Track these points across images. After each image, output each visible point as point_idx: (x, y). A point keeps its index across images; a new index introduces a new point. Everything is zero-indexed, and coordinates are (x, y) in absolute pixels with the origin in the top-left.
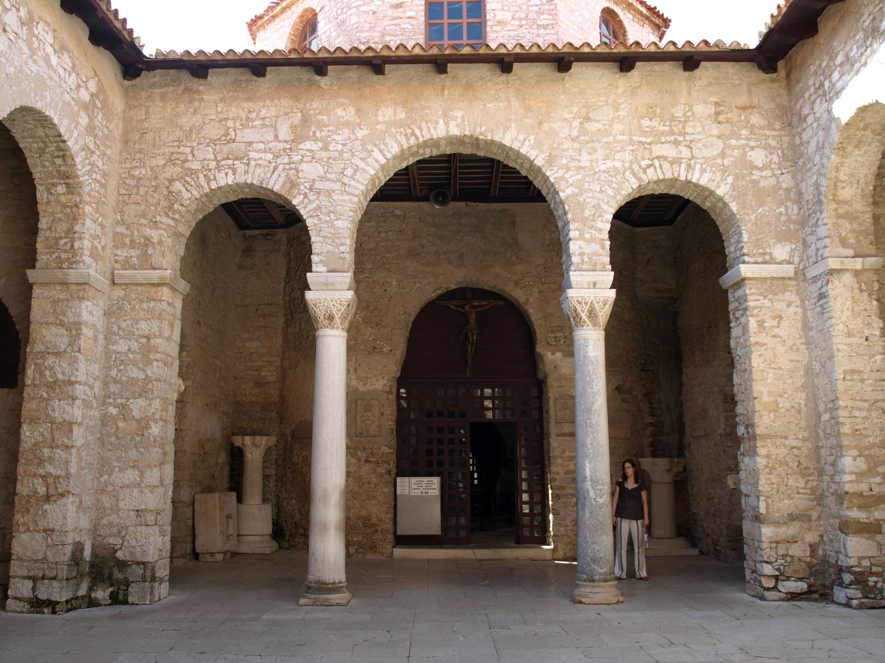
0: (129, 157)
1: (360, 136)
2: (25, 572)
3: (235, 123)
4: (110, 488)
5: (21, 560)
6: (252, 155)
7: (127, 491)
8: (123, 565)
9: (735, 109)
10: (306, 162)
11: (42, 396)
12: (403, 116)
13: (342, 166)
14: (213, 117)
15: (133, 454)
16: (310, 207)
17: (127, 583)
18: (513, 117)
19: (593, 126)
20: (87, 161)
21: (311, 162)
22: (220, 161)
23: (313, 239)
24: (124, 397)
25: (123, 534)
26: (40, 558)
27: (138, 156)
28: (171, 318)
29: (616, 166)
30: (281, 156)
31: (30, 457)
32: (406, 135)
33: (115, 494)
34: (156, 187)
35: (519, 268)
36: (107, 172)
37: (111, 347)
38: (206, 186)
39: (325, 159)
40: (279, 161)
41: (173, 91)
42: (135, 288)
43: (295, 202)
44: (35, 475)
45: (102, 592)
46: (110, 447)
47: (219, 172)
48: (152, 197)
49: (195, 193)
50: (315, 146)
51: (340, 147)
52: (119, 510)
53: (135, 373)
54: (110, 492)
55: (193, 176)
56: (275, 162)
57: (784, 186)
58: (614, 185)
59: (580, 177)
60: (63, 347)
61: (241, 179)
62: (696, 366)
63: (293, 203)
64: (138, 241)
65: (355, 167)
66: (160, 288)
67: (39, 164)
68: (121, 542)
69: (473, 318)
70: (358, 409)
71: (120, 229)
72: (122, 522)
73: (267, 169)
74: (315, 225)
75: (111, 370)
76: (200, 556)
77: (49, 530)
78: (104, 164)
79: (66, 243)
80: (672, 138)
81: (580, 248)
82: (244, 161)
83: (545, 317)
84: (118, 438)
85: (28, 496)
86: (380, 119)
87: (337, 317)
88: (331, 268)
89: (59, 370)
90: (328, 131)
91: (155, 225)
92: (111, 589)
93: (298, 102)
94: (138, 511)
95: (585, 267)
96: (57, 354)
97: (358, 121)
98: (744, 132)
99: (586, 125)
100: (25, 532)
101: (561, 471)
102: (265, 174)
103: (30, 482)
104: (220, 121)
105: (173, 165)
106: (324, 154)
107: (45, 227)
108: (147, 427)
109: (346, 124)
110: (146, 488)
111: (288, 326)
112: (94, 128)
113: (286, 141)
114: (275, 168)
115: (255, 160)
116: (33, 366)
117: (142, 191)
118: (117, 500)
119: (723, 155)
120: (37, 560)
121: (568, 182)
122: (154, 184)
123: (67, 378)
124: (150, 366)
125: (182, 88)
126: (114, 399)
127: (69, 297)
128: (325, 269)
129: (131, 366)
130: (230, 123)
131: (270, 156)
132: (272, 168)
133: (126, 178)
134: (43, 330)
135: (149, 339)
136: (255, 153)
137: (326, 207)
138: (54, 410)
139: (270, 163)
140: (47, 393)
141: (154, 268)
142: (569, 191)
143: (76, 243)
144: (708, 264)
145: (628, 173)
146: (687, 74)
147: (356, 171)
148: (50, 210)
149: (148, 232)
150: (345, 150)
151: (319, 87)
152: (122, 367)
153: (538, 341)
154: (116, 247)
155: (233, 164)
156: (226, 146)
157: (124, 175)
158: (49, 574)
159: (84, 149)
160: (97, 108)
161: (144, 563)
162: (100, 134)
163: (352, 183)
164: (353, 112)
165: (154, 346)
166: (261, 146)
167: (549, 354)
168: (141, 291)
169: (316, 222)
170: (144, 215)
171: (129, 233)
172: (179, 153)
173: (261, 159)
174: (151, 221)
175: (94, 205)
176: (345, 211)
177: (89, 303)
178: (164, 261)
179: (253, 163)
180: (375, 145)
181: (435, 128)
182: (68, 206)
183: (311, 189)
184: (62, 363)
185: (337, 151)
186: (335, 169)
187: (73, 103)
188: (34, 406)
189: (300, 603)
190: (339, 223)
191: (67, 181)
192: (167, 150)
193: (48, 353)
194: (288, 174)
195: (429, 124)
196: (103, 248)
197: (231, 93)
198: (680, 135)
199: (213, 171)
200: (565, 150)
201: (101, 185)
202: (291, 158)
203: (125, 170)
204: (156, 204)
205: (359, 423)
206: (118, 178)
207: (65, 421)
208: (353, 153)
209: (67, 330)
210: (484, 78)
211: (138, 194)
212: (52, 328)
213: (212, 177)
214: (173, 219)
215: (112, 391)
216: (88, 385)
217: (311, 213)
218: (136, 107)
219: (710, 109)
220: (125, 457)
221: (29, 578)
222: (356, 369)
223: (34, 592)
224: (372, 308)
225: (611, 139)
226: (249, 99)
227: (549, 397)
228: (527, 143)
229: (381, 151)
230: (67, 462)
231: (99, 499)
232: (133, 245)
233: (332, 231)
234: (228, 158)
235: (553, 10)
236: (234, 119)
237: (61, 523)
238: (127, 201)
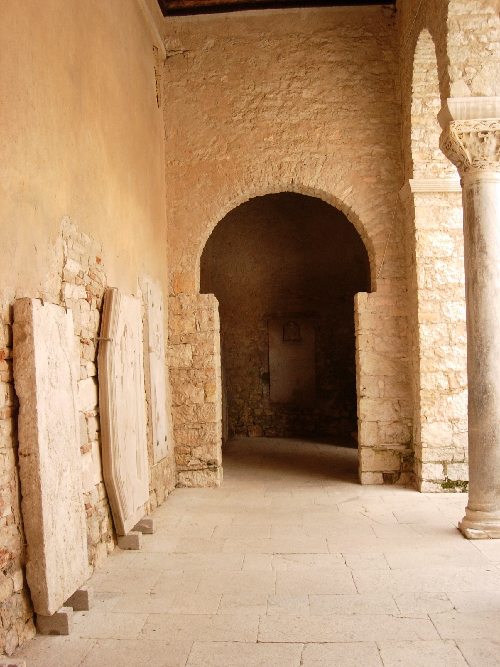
2: (437, 458)
5: (431, 447)
11: (435, 298)
26: (448, 444)
31: (432, 355)
44: (437, 371)
60: (450, 252)
67: (423, 79)
77: (455, 420)
85: (433, 390)
89: (448, 273)
96: (445, 259)
107: (417, 139)
116: (424, 271)
127: (448, 205)
134: (429, 236)
138: (448, 311)
140: (440, 295)
148: (424, 123)
184: (450, 267)
193: (437, 258)
212: (436, 234)
221: (440, 462)
223: (445, 475)
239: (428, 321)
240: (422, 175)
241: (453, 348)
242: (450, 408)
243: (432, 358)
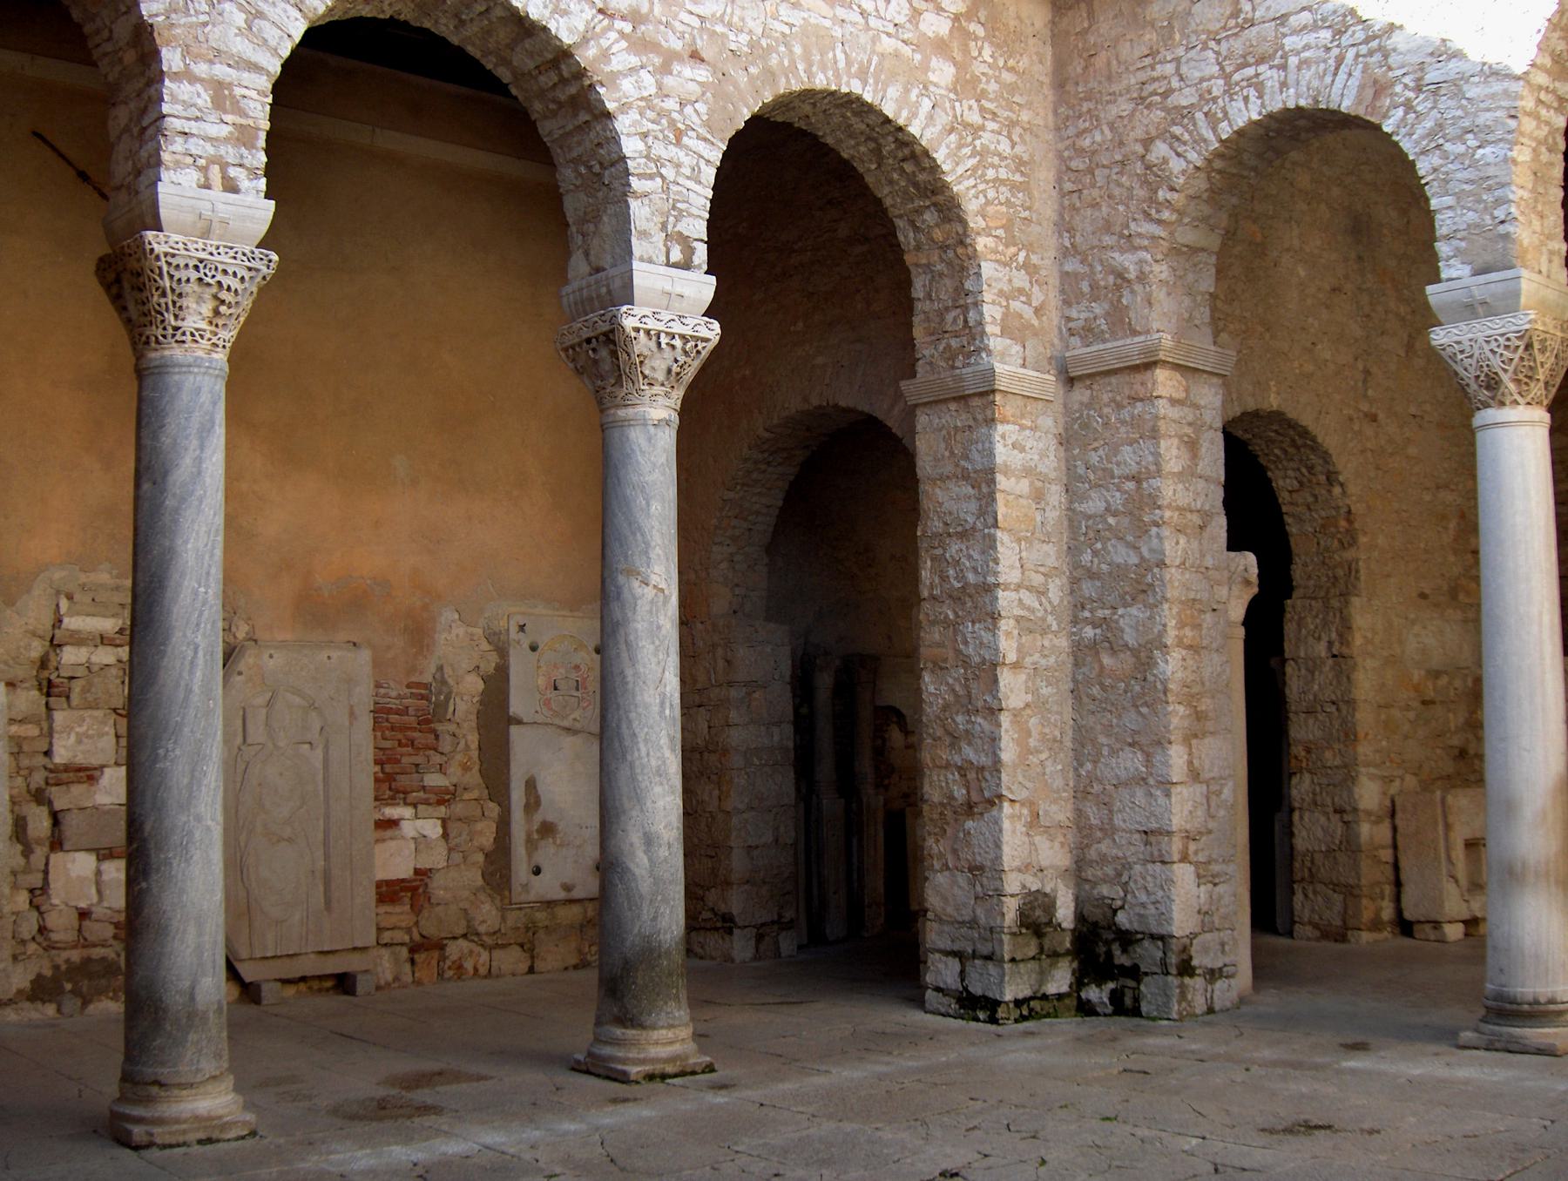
4: (1097, 788)
6: (1290, 42)
7: (1124, 793)
8: (1127, 939)
11: (947, 616)
15: (1131, 720)
16: (1419, 132)
17: (1135, 973)
20: (967, 151)
23: (1434, 203)
24: (1108, 605)
25: (1125, 878)
26: (967, 918)
27: (1085, 106)
28: (1188, 430)
31: (940, 732)
33: (1106, 800)
34: (1122, 162)
36: (1026, 157)
38: (1209, 135)
40: (1345, 40)
42: (1107, 380)
43: (1387, 129)
44: (947, 766)
45: (1097, 990)
46: (1092, 707)
47: (1232, 100)
48: (1119, 185)
49: (1193, 156)
52: (1114, 830)
53: (1122, 555)
55: (1186, 121)
56: (1338, 46)
61: (1275, 105)
64: (1102, 283)
66: (1149, 373)
68: (1122, 894)
71: (1072, 266)
72: (1120, 854)
74: (1435, 170)
75: (1081, 553)
76: (1416, 928)
78: (1013, 145)
79: (955, 320)
82: (1276, 62)
84: (1103, 688)
85: (941, 804)
87: (1505, 378)
89: (968, 564)
91: (1129, 242)
92: (1111, 985)
94: (1146, 832)
96: (964, 535)
100: (941, 871)
102: (1322, 78)
103: (942, 778)
107: (921, 295)
110: (1158, 788)
112: (975, 80)
114: (1340, 60)
115: (1298, 53)
116: (929, 563)
120: (963, 923)
122: (1118, 157)
123: (982, 579)
124: (1145, 538)
127: (971, 423)
128: (1467, 270)
131: (1325, 35)
132: (1331, 62)
134: (938, 491)
135: (1139, 482)
136: (1294, 38)
138: (966, 643)
139: (1328, 49)
140: (956, 613)
141: (1135, 333)
148: (924, 261)
152: (1099, 546)
154: (1067, 303)
155: (1257, 75)
157: (1066, 154)
158: (984, 949)
159: (952, 130)
160: (976, 39)
161: (1162, 938)
162: (993, 87)
165: (1150, 495)
166: (1306, 17)
169: (1436, 160)
170: (1107, 227)
172: (1154, 80)
173: (1307, 47)
174: (1121, 236)
175: (1000, 232)
176: (1496, 120)
177: (1010, 427)
178: (1154, 315)
179: (1293, 61)
182: (948, 247)
183: (1418, 89)
184: (972, 552)
187: (907, 51)
188: (937, 636)
189: (1461, 1042)
191: (934, 199)
192: (1133, 81)
194: (1366, 65)
196: (1037, 311)
199: (1220, 101)
201: (1014, 187)
203: (1068, 142)
207: (984, 661)
209: (973, 487)
211: (1093, 186)
212: (951, 485)
213: (1220, 115)
214: (1159, 222)
216: (1030, 589)
217: (1424, 143)
220: (1118, 726)
223: (962, 980)
230: (994, 740)
231: (1080, 811)
232: (1096, 293)
234: (1246, 65)
237: (992, 855)
239: (935, 664)
240: (928, 368)
241: (973, 719)
242: (969, 844)
243: (940, 738)
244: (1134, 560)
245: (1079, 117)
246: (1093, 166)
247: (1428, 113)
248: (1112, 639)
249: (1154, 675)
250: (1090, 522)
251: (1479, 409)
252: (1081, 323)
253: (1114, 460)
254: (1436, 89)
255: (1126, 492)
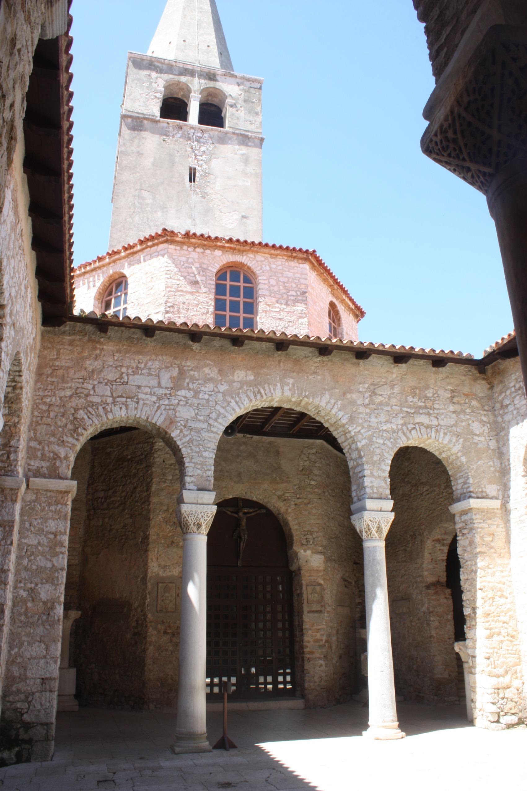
0: (42, 387)
1: (222, 391)
3: (128, 369)
4: (19, 660)
6: (141, 396)
9: (462, 395)
10: (182, 405)
12: (252, 378)
13: (209, 411)
14: (111, 363)
15: (40, 630)
16: (184, 440)
18: (326, 387)
19: (378, 399)
21: (185, 405)
22: (115, 398)
23: (187, 465)
27: (49, 387)
29: (393, 427)
30: (163, 398)
32: (254, 392)
33: (24, 665)
35: (283, 486)
37: (23, 540)
39: (196, 405)
40: (161, 402)
41: (80, 340)
43: (173, 435)
46: (20, 625)
50: (189, 394)
51: (206, 397)
53: (42, 562)
54: (19, 663)
55: (94, 407)
56: (159, 403)
57: (492, 448)
58: (392, 440)
59: (370, 433)
62: (398, 562)
63: (172, 435)
64: (48, 455)
65: (218, 413)
69: (244, 522)
70: (159, 590)
71: (33, 444)
73: (152, 407)
74: (188, 454)
80: (427, 411)
81: (371, 482)
82: (135, 400)
83: (299, 524)
86: (236, 378)
88: (200, 487)
90: (199, 384)
91: (63, 443)
93: (176, 359)
94: (43, 679)
95: (375, 496)
97: (220, 378)
98: (468, 411)
99: (374, 398)
101: (311, 640)
102: (151, 411)
104: (116, 367)
105: (78, 397)
106: (196, 401)
108: (53, 608)
109: (211, 380)
111: (90, 520)
113: (167, 388)
114: (159, 408)
117: (52, 414)
118: (26, 670)
119: (456, 425)
121: (363, 435)
122: (62, 410)
125: (87, 338)
126: (25, 584)
128: (196, 488)
129: (40, 557)
130: (124, 370)
131: (154, 399)
132: (156, 407)
133: (39, 403)
135: (56, 536)
136: (142, 394)
137: (197, 441)
142: (364, 442)
143: (12, 455)
144: (413, 490)
145: (400, 432)
146: (434, 369)
147: (218, 416)
149: (56, 448)
150: (211, 399)
151: (192, 350)
152: (32, 558)
153: (295, 542)
154: (29, 458)
156: (121, 387)
157: (37, 401)
163: (216, 424)
164: (216, 372)
165: (60, 541)
166: (148, 390)
167: (302, 551)
168: (50, 496)
169: (189, 451)
170: (53, 435)
171: (40, 447)
172: (83, 388)
173: (147, 399)
179: (141, 402)
180: (232, 398)
181: (274, 390)
183: (185, 427)
185: (204, 399)
186: (203, 413)
190: (206, 454)
192: (73, 385)
195: (271, 386)
197: (125, 347)
198: (431, 409)
200: (360, 413)
202: (171, 401)
203: (38, 397)
204: (63, 426)
205: (159, 602)
206: (32, 403)
208: (216, 402)
210: (307, 357)
213: (109, 410)
215: (23, 577)
218: (49, 348)
219: (448, 393)
220: (33, 633)
222: (157, 559)
224: (171, 511)
225: (389, 408)
226: (139, 353)
227: (302, 584)
228: (336, 406)
229: (236, 402)
232: (43, 458)
233: (201, 459)
234: (121, 396)
235: (305, 300)
236: (128, 367)
238: (40, 422)
244: (49, 565)
245: (46, 389)
246: (50, 409)
247: (187, 435)
248: (34, 597)
249: (55, 613)
250: (30, 547)
251: (190, 533)
252: (34, 468)
253: (45, 524)
254: (191, 429)
255: (49, 538)
